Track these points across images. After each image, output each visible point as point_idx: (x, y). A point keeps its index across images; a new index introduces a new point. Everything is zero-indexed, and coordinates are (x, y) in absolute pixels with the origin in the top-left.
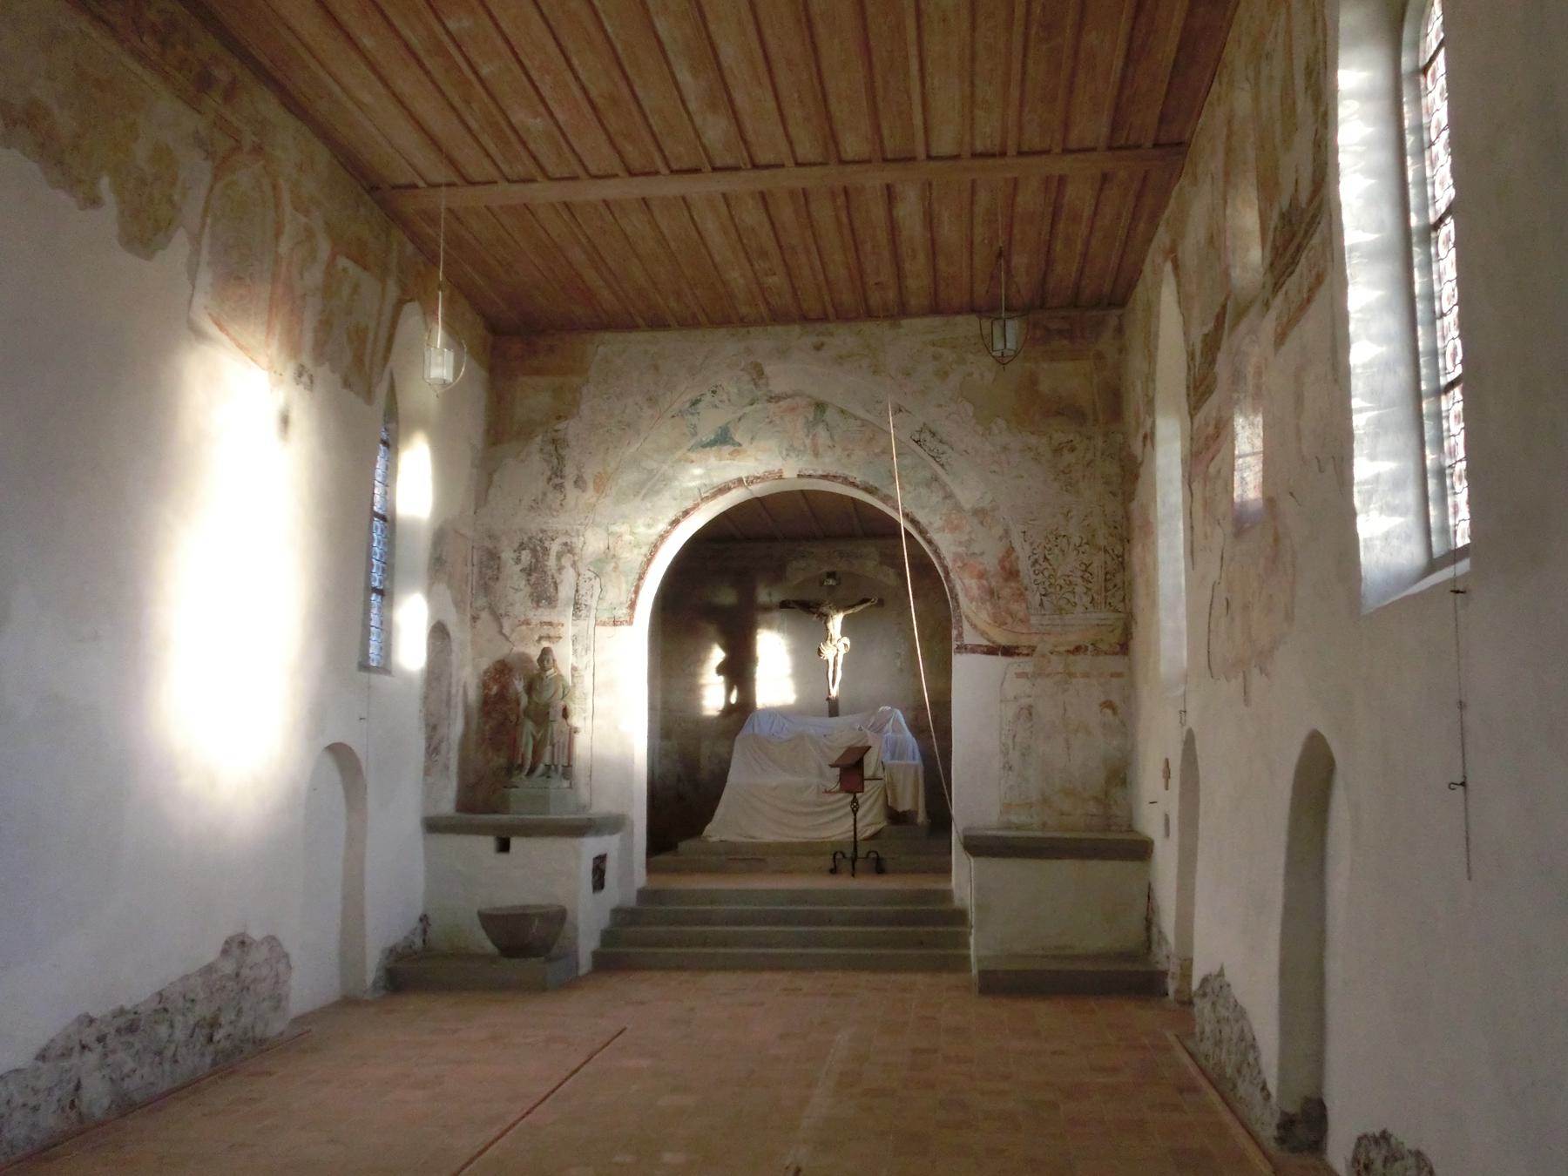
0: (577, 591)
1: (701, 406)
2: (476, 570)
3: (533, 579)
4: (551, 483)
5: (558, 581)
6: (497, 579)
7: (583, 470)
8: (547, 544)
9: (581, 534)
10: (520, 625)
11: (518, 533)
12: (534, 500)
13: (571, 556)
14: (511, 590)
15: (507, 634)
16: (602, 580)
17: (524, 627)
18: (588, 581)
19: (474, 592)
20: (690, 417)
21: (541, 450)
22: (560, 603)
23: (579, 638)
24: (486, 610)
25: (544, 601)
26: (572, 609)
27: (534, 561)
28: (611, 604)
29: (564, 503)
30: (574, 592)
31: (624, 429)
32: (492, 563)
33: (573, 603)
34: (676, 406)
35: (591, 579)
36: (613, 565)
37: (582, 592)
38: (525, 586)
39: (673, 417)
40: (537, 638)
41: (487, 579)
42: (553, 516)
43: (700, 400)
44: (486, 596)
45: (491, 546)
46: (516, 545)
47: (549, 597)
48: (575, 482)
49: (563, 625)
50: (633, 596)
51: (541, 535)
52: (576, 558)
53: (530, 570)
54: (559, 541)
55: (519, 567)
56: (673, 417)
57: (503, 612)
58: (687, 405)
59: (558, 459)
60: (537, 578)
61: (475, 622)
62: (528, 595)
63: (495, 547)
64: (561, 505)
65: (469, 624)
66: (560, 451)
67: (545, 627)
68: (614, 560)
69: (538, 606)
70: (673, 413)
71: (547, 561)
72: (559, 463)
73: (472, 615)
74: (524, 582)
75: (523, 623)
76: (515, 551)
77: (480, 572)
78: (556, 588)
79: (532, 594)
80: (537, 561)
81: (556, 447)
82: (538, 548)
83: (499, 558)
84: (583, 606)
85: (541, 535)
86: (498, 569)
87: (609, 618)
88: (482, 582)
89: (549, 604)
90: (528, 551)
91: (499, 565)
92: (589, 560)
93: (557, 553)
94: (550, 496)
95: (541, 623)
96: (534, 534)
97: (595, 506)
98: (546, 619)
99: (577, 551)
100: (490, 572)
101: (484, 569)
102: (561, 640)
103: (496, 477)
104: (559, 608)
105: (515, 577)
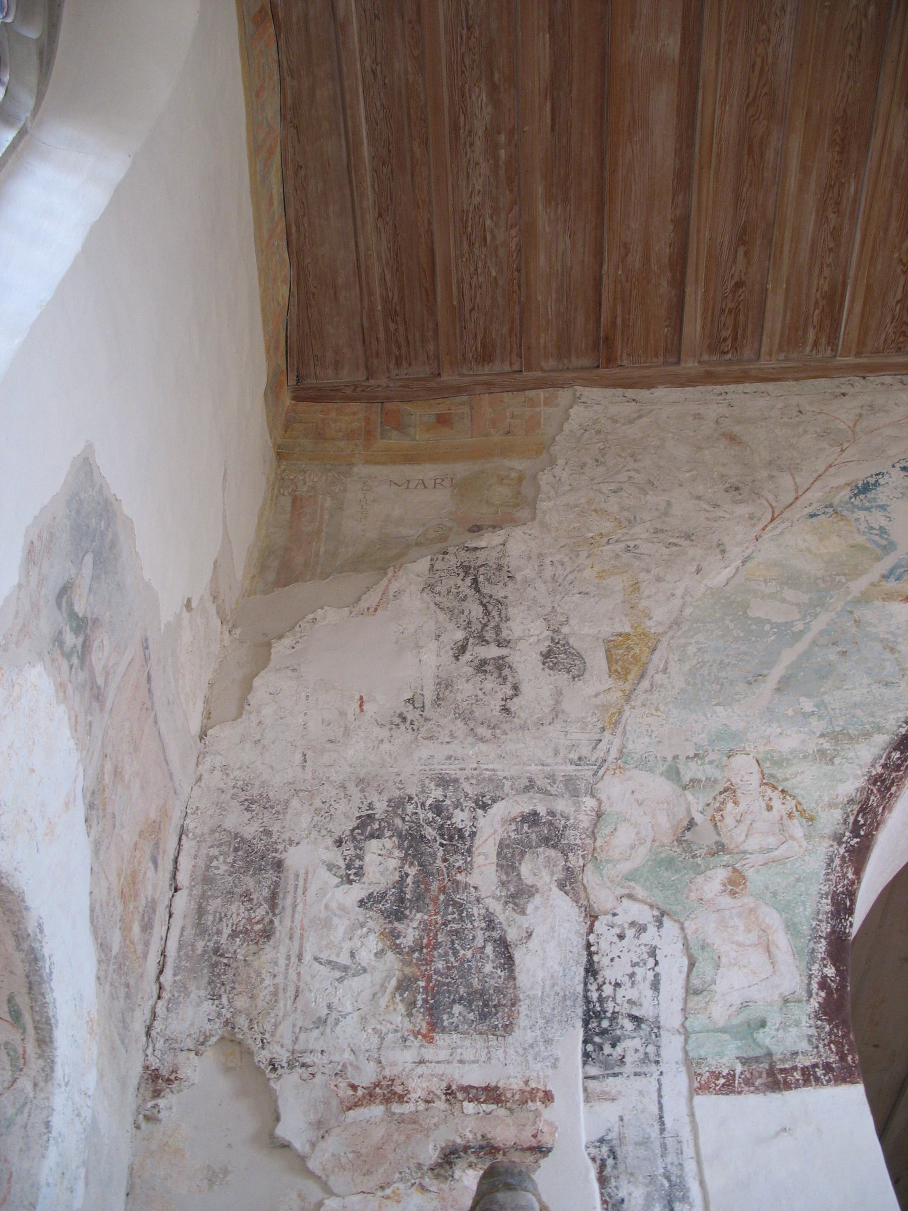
0: (591, 970)
1: (881, 495)
2: (182, 902)
3: (410, 934)
4: (467, 657)
5: (512, 935)
6: (267, 934)
7: (565, 630)
8: (460, 818)
9: (582, 786)
10: (355, 1105)
11: (352, 789)
12: (411, 701)
13: (552, 853)
14: (324, 970)
15: (299, 1144)
16: (690, 926)
17: (377, 1111)
18: (630, 933)
19: (168, 978)
20: (861, 514)
21: (430, 587)
22: (524, 1015)
23: (629, 1153)
24: (209, 1054)
25: (457, 1009)
26: (580, 1034)
27: (412, 871)
28: (745, 1005)
29: (513, 705)
30: (580, 972)
31: (675, 545)
32: (249, 882)
33: (580, 1011)
34: (815, 495)
35: (642, 929)
36: (721, 875)
37: (610, 973)
38: (379, 954)
39: (812, 516)
40: (430, 1154)
41: (223, 939)
42: (482, 739)
43: (876, 484)
44: (215, 997)
45: (250, 831)
46: (344, 825)
47: (482, 993)
48: (546, 655)
49: (548, 1097)
50: (830, 971)
51: (438, 793)
52: (575, 861)
53: (401, 900)
54: (499, 810)
55: (357, 891)
56: (812, 516)
57: (283, 1056)
58: (846, 493)
59: (485, 606)
60: (426, 927)
61: (157, 1094)
62: (394, 982)
63: (268, 833)
64: (506, 710)
65: (131, 1100)
66: (486, 589)
67: (469, 1107)
68: (726, 858)
69: (435, 1026)
70: (809, 510)
71: (467, 869)
72: (487, 613)
73: (147, 1068)
74: (373, 943)
75: (370, 1096)
76: (339, 843)
77: (201, 912)
78: (507, 960)
79: (405, 984)
80: (425, 872)
81: (475, 581)
82: (430, 832)
83: (279, 865)
84: (629, 1025)
85: (438, 793)
86: (273, 900)
87: (745, 1061)
88: (200, 945)
89: (483, 1017)
90: (388, 843)
91: (277, 884)
92: (625, 867)
93: (501, 846)
94: (466, 689)
95: (449, 1092)
96: (412, 791)
97: (620, 713)
98: (475, 1077)
99: (572, 837)
100: (237, 911)
101: (214, 905)
102: (543, 1162)
103: (280, 649)
104: (523, 1033)
105: (341, 926)
